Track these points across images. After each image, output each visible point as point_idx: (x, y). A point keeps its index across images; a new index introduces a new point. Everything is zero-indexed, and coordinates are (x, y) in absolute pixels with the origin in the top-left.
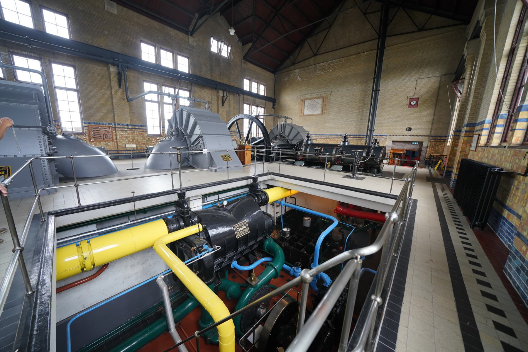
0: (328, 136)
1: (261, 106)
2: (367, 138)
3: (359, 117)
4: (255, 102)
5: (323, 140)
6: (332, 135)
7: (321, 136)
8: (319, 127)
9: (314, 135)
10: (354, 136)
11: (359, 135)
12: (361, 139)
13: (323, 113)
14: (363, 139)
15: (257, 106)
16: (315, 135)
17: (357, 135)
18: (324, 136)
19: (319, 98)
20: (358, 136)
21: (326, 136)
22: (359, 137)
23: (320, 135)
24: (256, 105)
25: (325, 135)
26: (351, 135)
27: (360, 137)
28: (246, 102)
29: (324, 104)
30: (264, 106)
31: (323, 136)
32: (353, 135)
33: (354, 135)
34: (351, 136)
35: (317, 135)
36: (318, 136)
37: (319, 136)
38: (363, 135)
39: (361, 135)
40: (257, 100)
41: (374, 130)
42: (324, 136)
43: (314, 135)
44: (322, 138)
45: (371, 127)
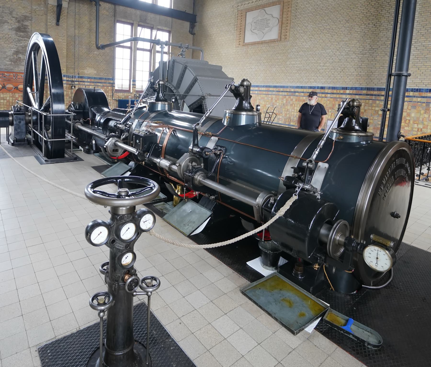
0: (292, 90)
1: (159, 27)
2: (387, 96)
3: (368, 41)
4: (146, 19)
5: (283, 99)
6: (302, 87)
7: (277, 89)
8: (274, 69)
9: (263, 87)
10: (355, 92)
11: (368, 89)
12: (374, 97)
13: (282, 37)
14: (378, 98)
15: (152, 28)
16: (267, 87)
17: (362, 89)
18: (285, 89)
19: (273, 4)
20: (364, 92)
21: (288, 90)
22: (369, 92)
23: (275, 87)
24: (149, 25)
25: (287, 87)
26: (346, 88)
27: (372, 92)
28: (123, 20)
29: (284, 16)
30: (168, 29)
31: (282, 89)
32: (352, 89)
33: (356, 89)
34: (348, 91)
35: (270, 87)
36: (271, 89)
37: (275, 89)
38: (379, 89)
39: (373, 89)
40: (151, 16)
41: (409, 75)
42: (285, 89)
43: (263, 87)
44: (281, 93)
45: (400, 68)
